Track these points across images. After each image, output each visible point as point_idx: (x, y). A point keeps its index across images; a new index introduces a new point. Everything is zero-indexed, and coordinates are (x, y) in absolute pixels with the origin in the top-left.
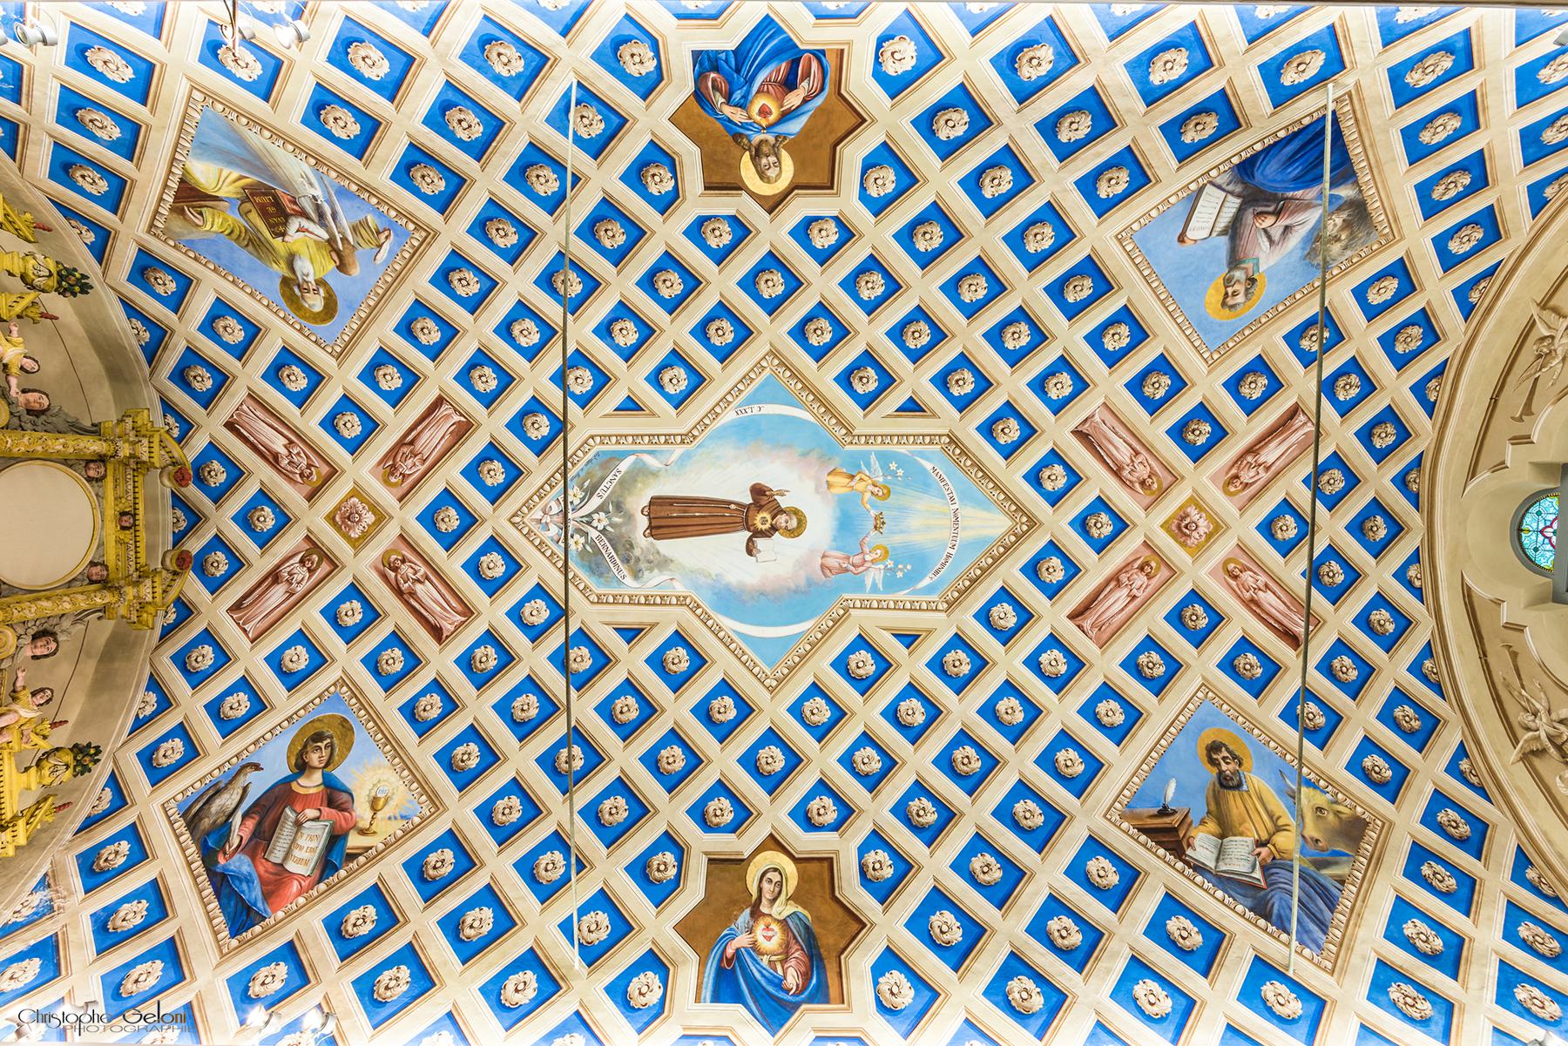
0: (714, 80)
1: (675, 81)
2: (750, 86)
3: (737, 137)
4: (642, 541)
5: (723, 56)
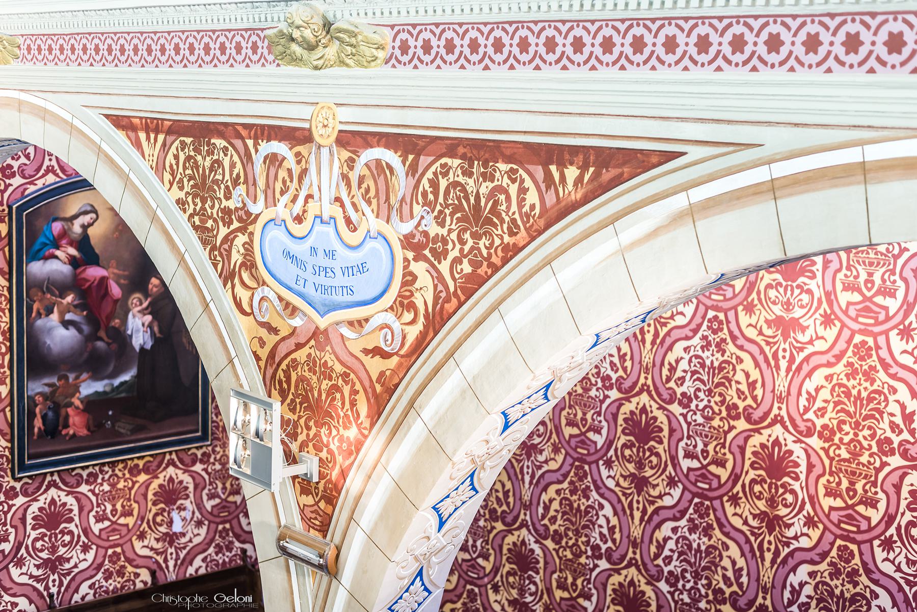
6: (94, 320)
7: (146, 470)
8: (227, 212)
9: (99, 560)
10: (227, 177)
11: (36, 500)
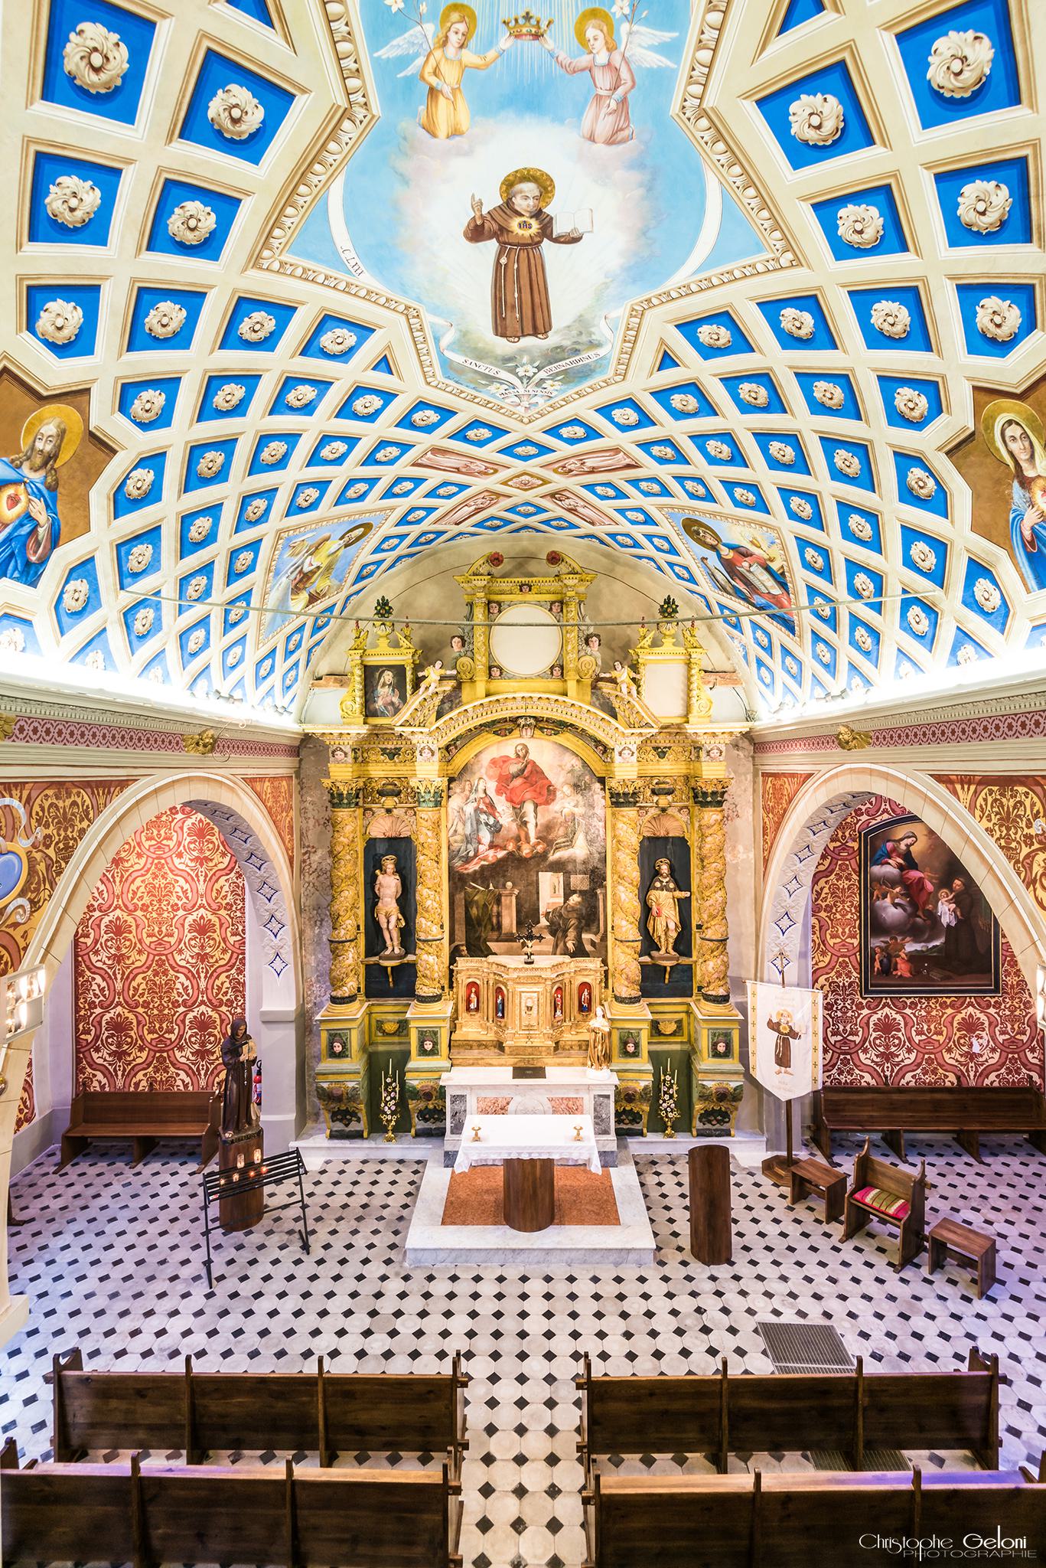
0: (35, 552)
1: (63, 564)
2: (10, 534)
3: (53, 488)
4: (553, 339)
5: (16, 574)
6: (914, 904)
7: (952, 1006)
8: (1030, 837)
9: (919, 1061)
10: (1028, 812)
11: (875, 1013)
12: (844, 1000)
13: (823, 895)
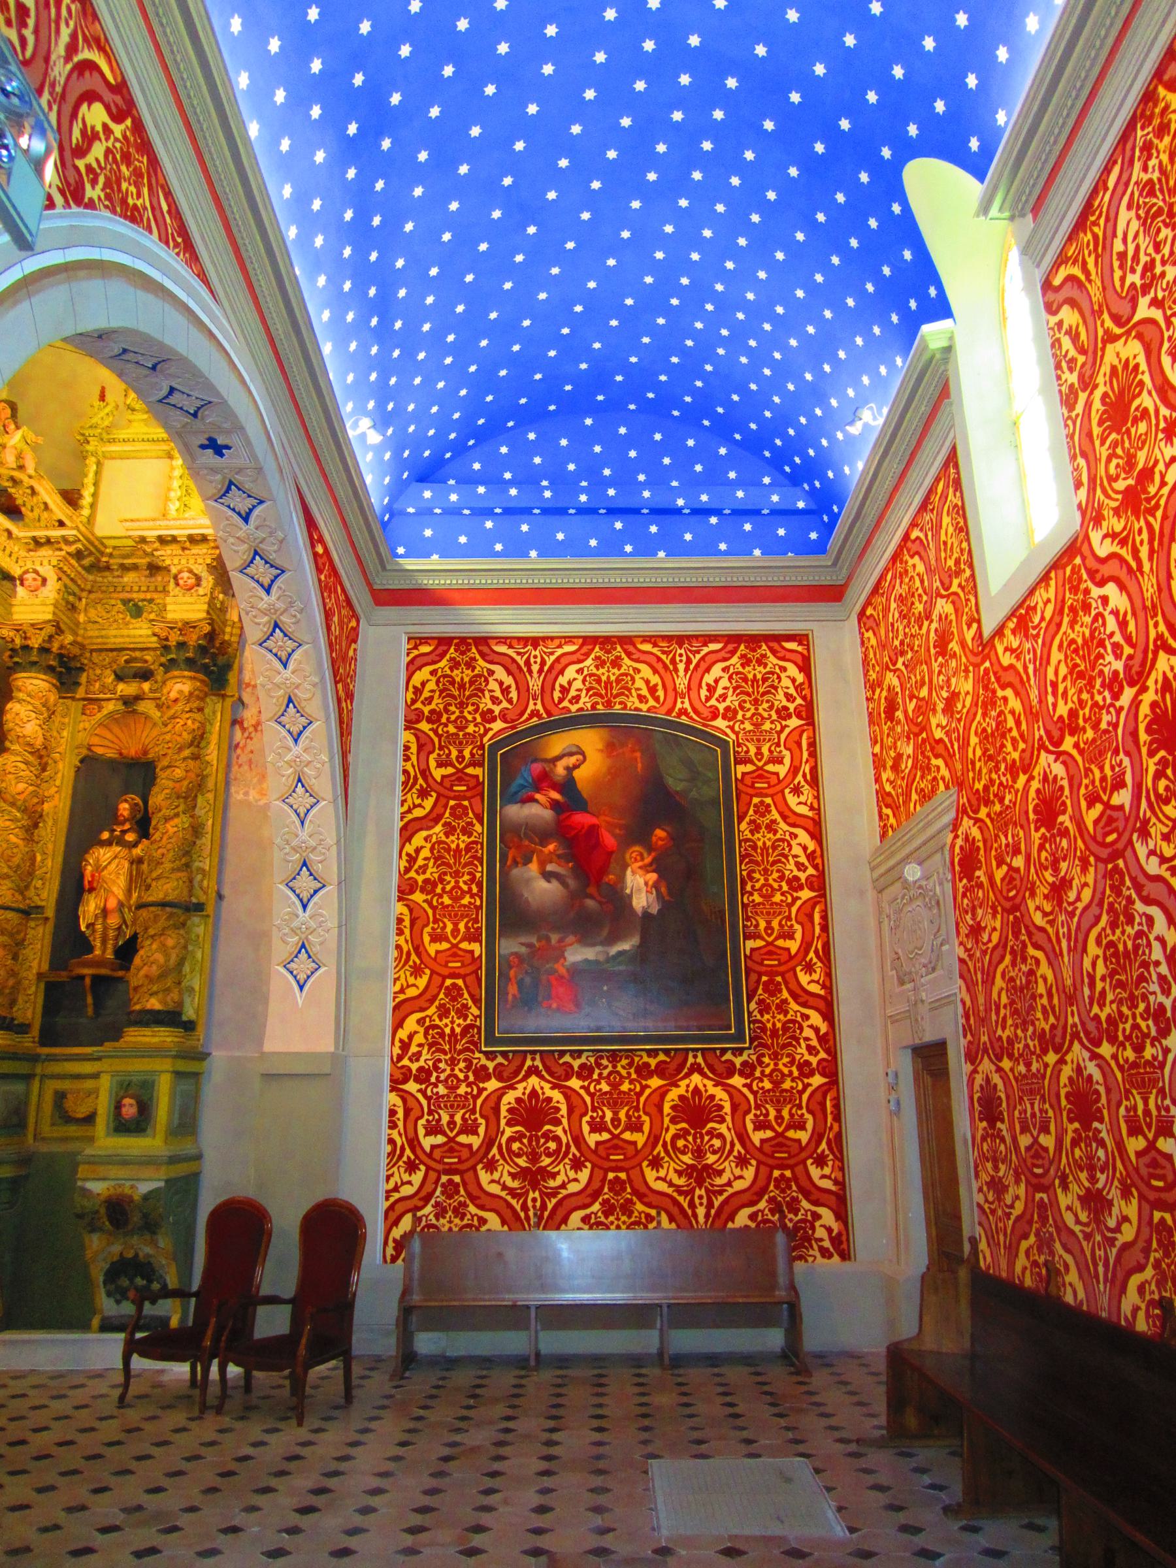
7: (660, 1071)
11: (512, 1087)
12: (453, 1063)
13: (420, 862)
